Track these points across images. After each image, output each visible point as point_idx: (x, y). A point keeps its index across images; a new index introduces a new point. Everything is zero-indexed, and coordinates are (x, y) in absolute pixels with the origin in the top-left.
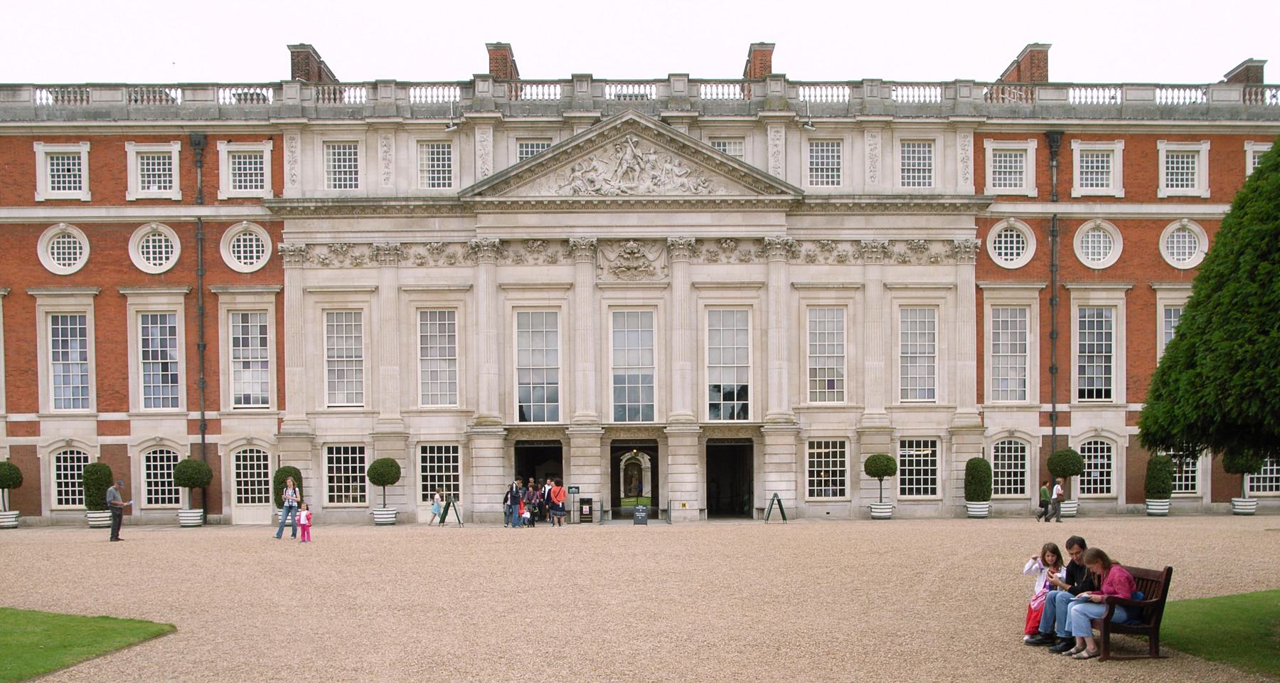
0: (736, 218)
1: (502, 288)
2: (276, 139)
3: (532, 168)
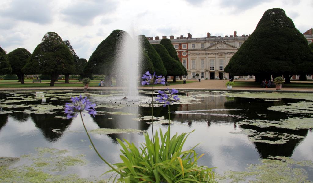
0: (232, 50)
1: (209, 57)
2: (187, 44)
3: (212, 46)
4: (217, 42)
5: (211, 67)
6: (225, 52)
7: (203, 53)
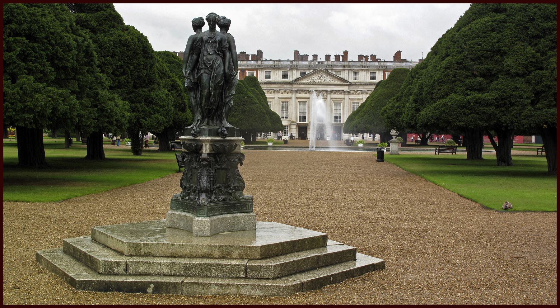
0: (339, 87)
1: (297, 98)
2: (257, 70)
3: (303, 77)
4: (312, 71)
5: (300, 117)
6: (327, 89)
7: (285, 89)
